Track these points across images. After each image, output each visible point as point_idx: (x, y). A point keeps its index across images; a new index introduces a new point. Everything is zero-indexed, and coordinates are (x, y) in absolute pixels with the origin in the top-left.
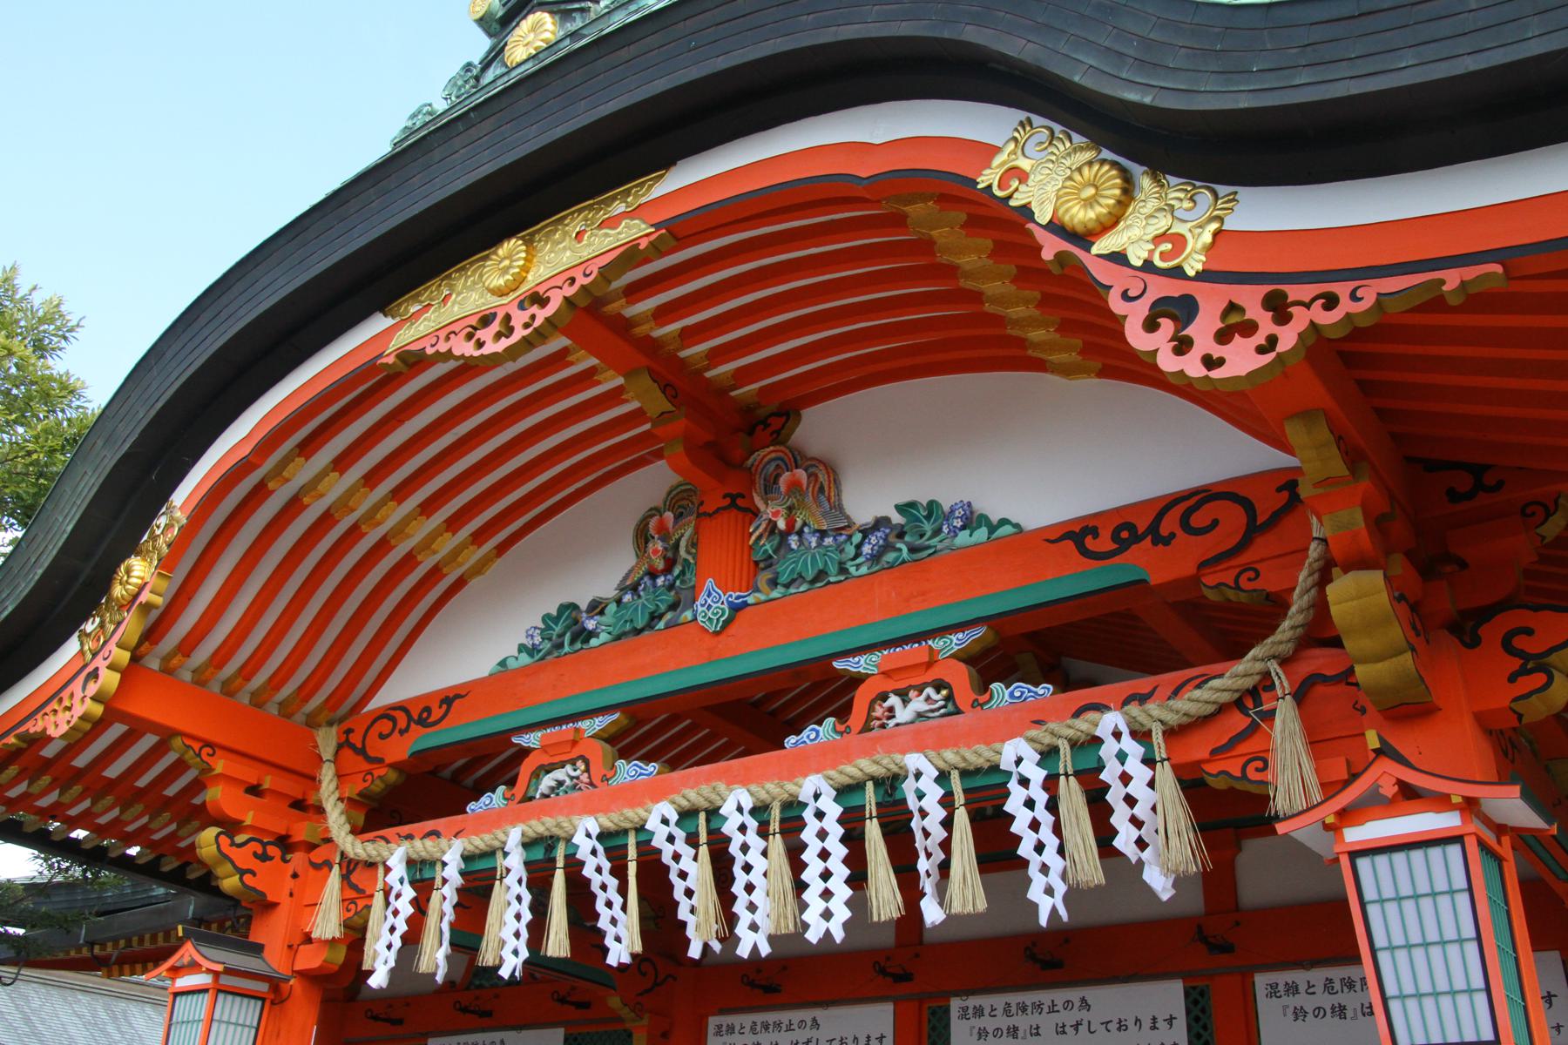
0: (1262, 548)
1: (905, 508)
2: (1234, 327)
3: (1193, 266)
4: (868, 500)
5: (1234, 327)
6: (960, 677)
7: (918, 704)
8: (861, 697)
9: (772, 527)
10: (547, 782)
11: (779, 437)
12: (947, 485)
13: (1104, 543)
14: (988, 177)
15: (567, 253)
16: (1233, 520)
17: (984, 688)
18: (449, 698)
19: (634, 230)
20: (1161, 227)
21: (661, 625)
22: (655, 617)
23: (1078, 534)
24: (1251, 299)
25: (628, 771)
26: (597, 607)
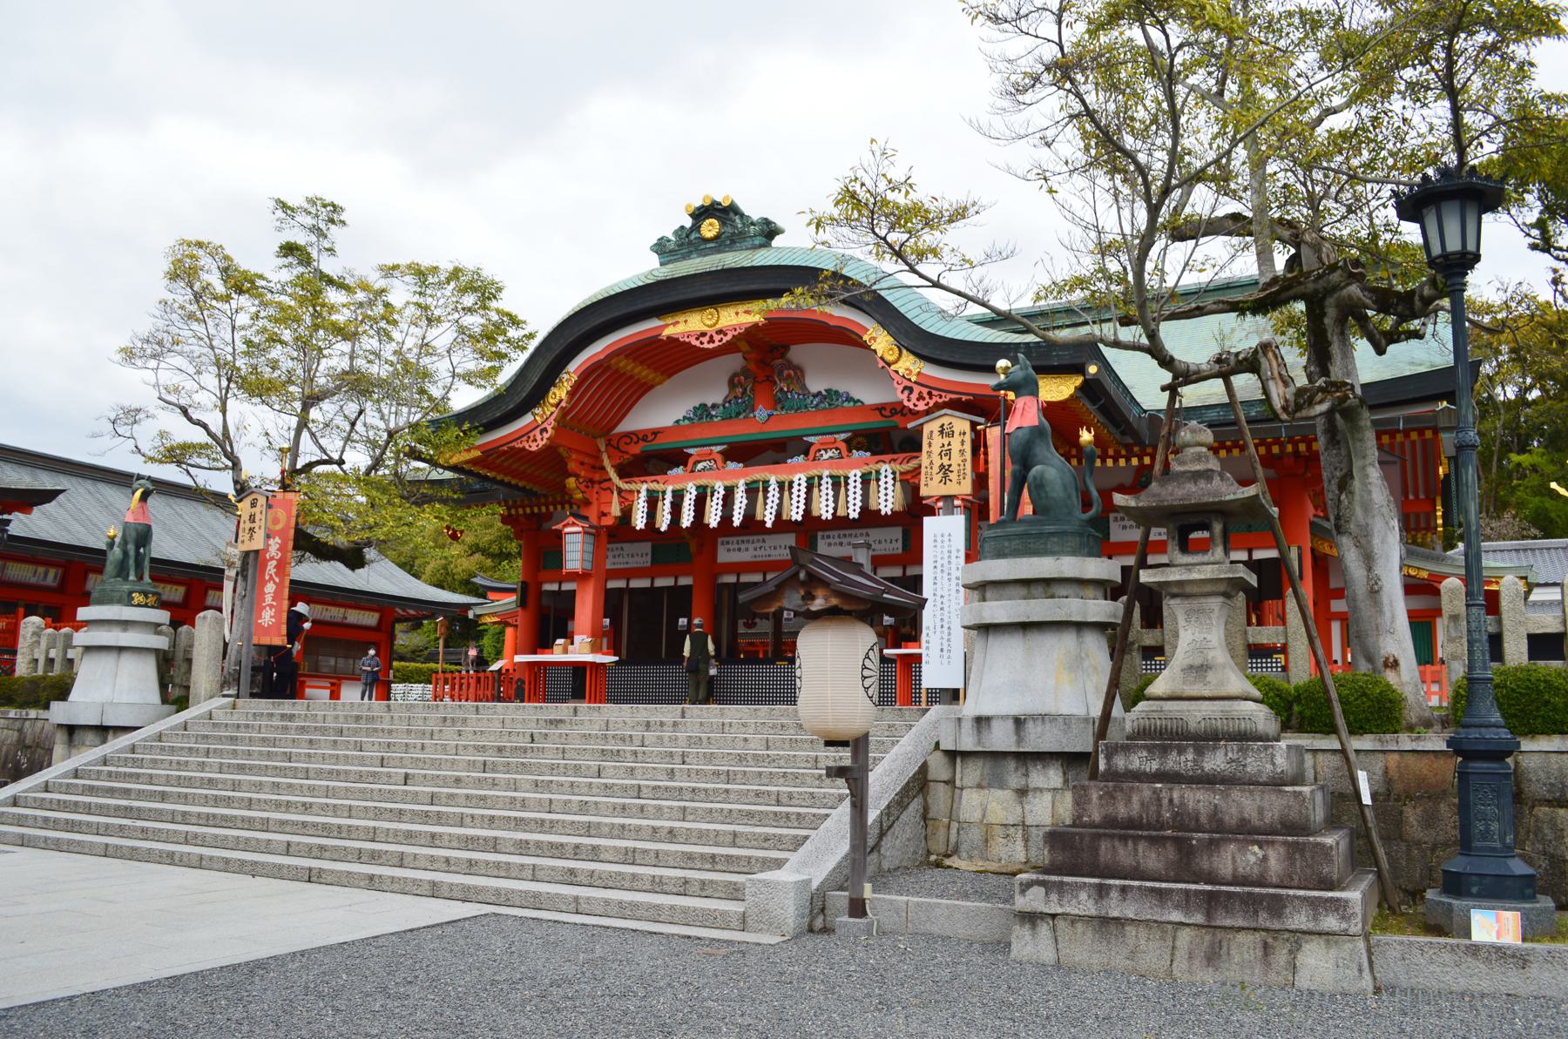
2: (921, 398)
3: (914, 379)
4: (815, 385)
5: (921, 398)
6: (843, 447)
7: (830, 454)
10: (700, 466)
11: (783, 356)
12: (841, 387)
13: (887, 413)
14: (866, 338)
17: (850, 451)
18: (656, 433)
20: (908, 365)
22: (738, 414)
23: (880, 408)
24: (925, 391)
25: (731, 466)
26: (714, 406)
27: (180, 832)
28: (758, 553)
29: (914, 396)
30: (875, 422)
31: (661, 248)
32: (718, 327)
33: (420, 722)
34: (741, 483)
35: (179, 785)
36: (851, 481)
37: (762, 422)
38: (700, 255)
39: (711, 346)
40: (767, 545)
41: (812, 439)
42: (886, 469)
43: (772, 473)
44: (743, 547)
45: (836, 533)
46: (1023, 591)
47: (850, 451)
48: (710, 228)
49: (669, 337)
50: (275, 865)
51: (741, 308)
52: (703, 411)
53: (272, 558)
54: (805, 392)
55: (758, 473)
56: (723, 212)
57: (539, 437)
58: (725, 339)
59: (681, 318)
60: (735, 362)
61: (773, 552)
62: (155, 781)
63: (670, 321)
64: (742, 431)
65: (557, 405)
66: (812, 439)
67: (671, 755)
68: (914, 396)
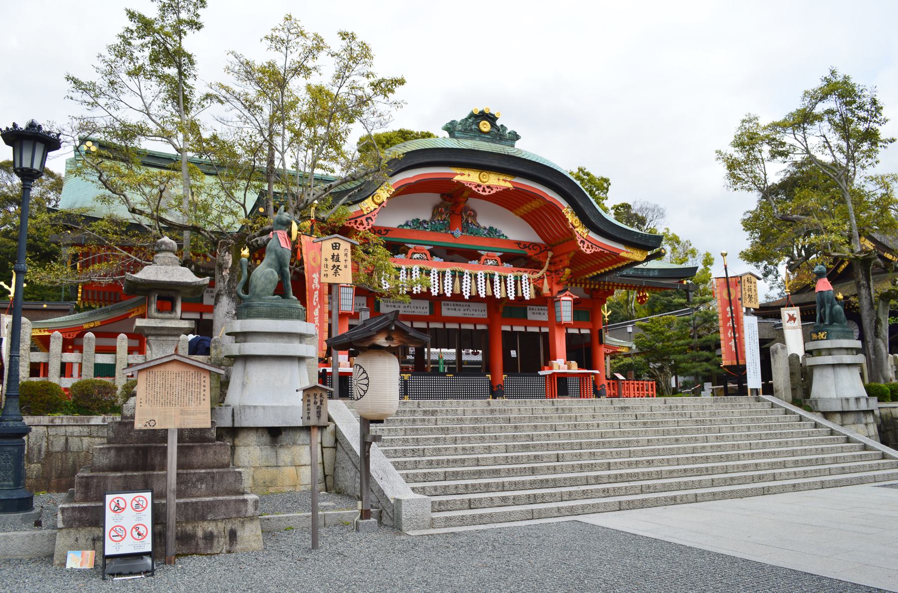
0: (541, 255)
1: (491, 228)
2: (588, 247)
5: (588, 247)
6: (499, 260)
8: (483, 258)
9: (467, 221)
10: (416, 256)
15: (497, 182)
16: (537, 251)
19: (509, 185)
20: (581, 231)
21: (443, 231)
23: (518, 243)
26: (425, 222)
27: (636, 487)
28: (406, 309)
29: (585, 246)
30: (516, 250)
31: (451, 129)
32: (487, 184)
33: (541, 412)
34: (448, 270)
35: (507, 463)
36: (479, 277)
37: (458, 238)
38: (481, 140)
39: (484, 194)
40: (471, 308)
41: (482, 252)
42: (525, 276)
43: (497, 270)
44: (457, 308)
45: (452, 303)
46: (845, 352)
47: (502, 262)
48: (485, 126)
49: (458, 182)
50: (744, 490)
51: (502, 177)
52: (418, 223)
53: (316, 289)
54: (479, 226)
55: (458, 267)
56: (492, 119)
57: (365, 223)
58: (492, 192)
59: (466, 172)
60: (436, 198)
61: (415, 310)
62: (481, 463)
63: (458, 171)
64: (444, 240)
65: (379, 205)
66: (482, 252)
67: (726, 420)
68: (585, 246)
